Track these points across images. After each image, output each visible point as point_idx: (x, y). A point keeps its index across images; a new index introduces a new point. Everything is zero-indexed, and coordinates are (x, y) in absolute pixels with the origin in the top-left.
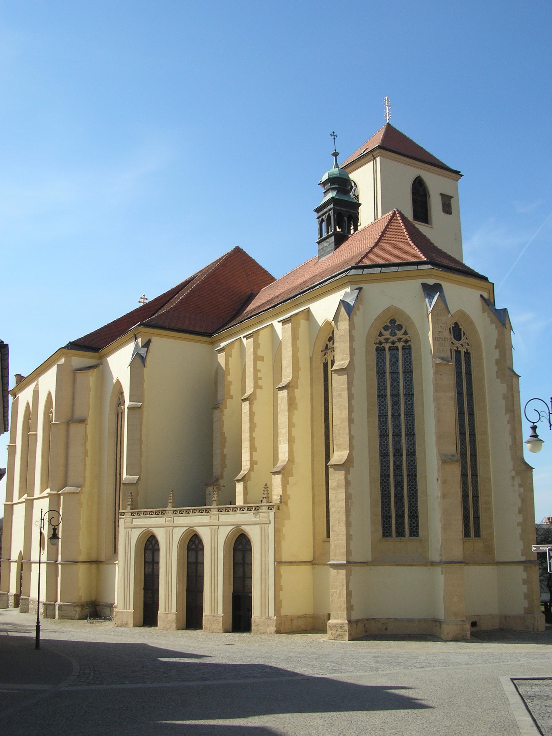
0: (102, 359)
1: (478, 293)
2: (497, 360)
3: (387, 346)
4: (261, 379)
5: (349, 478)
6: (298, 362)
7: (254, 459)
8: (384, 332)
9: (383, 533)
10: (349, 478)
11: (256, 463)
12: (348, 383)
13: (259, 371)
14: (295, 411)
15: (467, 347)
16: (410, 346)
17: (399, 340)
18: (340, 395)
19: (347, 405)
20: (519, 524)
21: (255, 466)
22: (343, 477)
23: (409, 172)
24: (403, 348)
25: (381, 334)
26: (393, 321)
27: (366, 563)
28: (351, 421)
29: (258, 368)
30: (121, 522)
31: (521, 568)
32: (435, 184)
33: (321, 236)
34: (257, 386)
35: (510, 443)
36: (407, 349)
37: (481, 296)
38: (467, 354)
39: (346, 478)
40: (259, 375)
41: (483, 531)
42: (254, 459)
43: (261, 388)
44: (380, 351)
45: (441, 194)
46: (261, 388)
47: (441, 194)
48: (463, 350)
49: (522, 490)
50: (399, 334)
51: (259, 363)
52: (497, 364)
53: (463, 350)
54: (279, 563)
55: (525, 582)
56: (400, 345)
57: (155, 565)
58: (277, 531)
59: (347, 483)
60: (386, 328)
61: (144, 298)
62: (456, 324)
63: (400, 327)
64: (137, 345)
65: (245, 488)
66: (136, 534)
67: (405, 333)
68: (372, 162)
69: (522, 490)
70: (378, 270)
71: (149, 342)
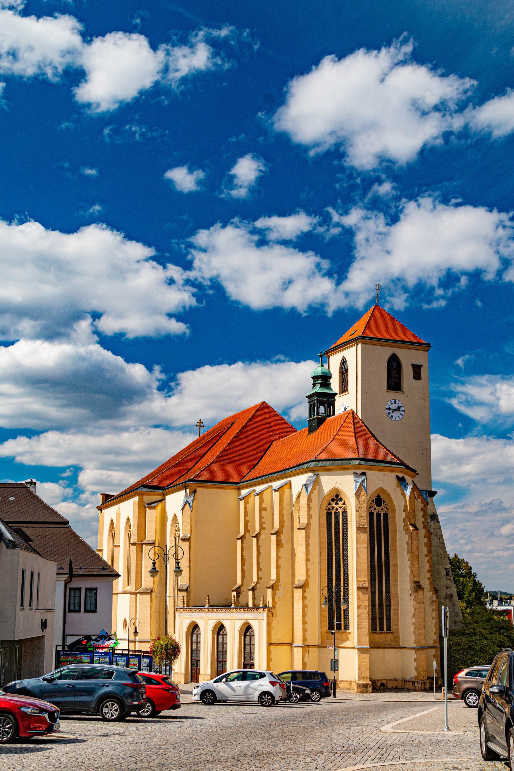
0: (164, 495)
1: (394, 474)
2: (404, 519)
3: (333, 512)
4: (264, 523)
5: (306, 594)
6: (283, 517)
7: (260, 576)
8: (331, 502)
9: (329, 627)
10: (306, 594)
11: (261, 578)
12: (306, 536)
13: (263, 518)
14: (281, 549)
15: (386, 510)
16: (347, 512)
17: (340, 507)
18: (301, 544)
19: (305, 550)
20: (413, 624)
21: (260, 580)
22: (301, 595)
23: (386, 352)
24: (343, 512)
25: (330, 504)
26: (337, 496)
27: (318, 646)
28: (307, 560)
29: (263, 516)
30: (177, 615)
31: (413, 651)
32: (408, 358)
33: (310, 417)
34: (261, 528)
35: (409, 573)
36: (345, 513)
37: (397, 476)
38: (386, 515)
39: (303, 595)
40: (263, 520)
41: (393, 628)
42: (260, 576)
43: (264, 529)
44: (329, 514)
45: (413, 365)
46: (264, 529)
47: (413, 365)
48: (382, 512)
49: (415, 602)
50: (340, 503)
51: (263, 512)
52: (404, 522)
53: (382, 512)
54: (270, 644)
55: (415, 660)
56: (341, 511)
57: (198, 644)
58: (269, 624)
59: (304, 598)
60: (333, 500)
61: (200, 423)
62: (378, 496)
63: (341, 499)
64: (186, 495)
65: (254, 594)
66: (186, 623)
67: (344, 504)
68: (356, 347)
69: (415, 602)
70: (328, 463)
71: (195, 492)
